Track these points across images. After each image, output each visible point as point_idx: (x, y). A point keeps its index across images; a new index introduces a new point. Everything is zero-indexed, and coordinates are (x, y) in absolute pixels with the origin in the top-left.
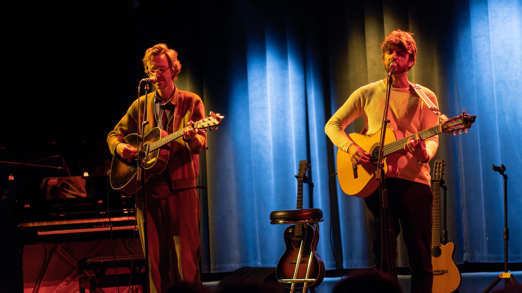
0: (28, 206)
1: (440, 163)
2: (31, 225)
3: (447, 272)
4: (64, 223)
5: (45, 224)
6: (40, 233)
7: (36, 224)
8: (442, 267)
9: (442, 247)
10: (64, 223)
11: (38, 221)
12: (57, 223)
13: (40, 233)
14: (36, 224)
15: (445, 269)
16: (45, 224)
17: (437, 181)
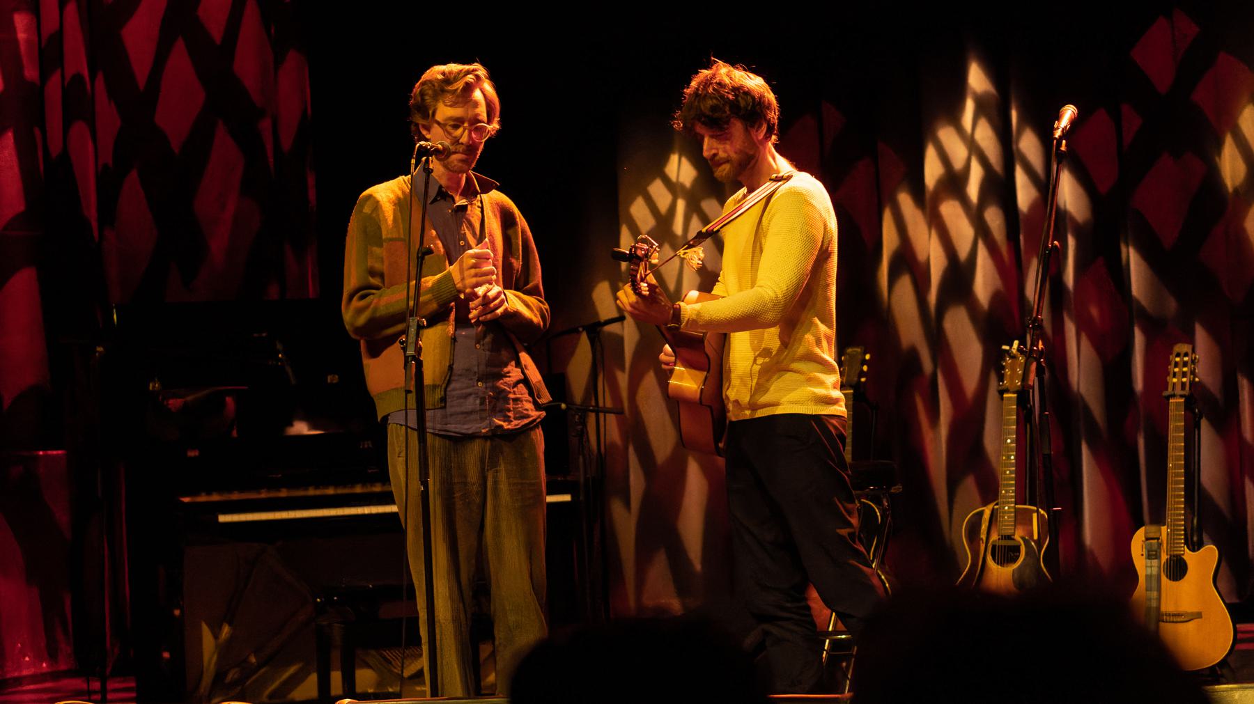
0: (192, 454)
1: (1186, 355)
2: (203, 498)
3: (1198, 615)
4: (284, 493)
5: (236, 496)
6: (223, 518)
7: (215, 497)
8: (1187, 606)
9: (1189, 556)
10: (284, 493)
11: (220, 490)
12: (264, 495)
13: (223, 518)
14: (215, 497)
15: (1195, 610)
16: (236, 496)
17: (1181, 396)
